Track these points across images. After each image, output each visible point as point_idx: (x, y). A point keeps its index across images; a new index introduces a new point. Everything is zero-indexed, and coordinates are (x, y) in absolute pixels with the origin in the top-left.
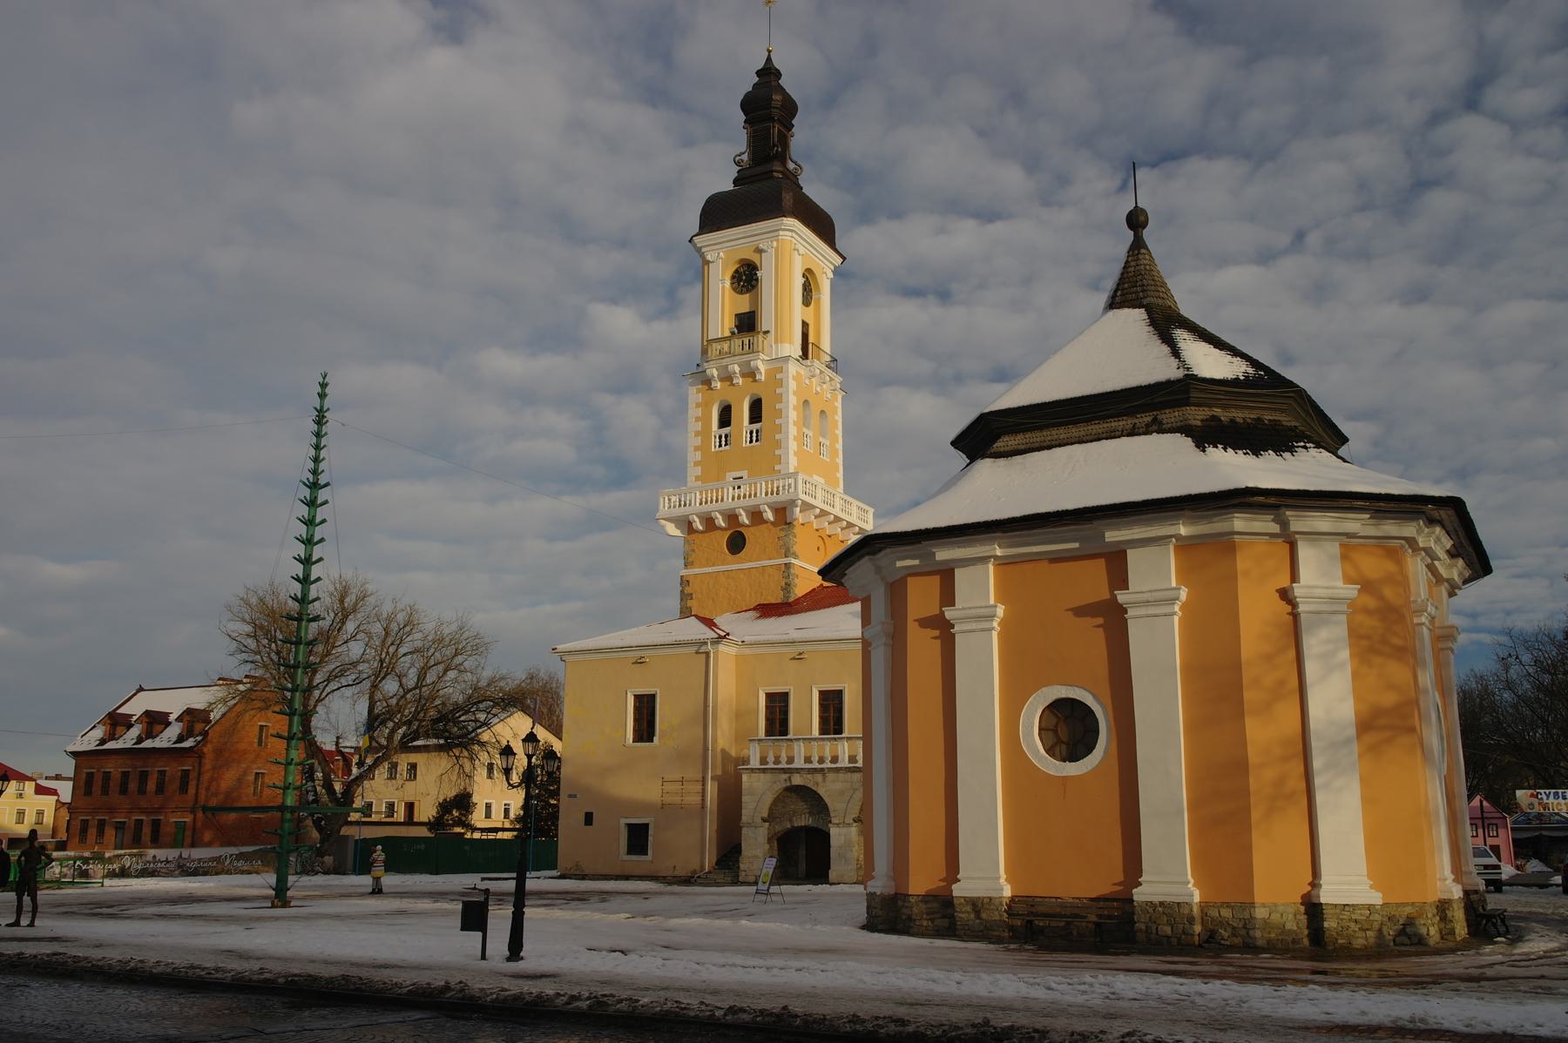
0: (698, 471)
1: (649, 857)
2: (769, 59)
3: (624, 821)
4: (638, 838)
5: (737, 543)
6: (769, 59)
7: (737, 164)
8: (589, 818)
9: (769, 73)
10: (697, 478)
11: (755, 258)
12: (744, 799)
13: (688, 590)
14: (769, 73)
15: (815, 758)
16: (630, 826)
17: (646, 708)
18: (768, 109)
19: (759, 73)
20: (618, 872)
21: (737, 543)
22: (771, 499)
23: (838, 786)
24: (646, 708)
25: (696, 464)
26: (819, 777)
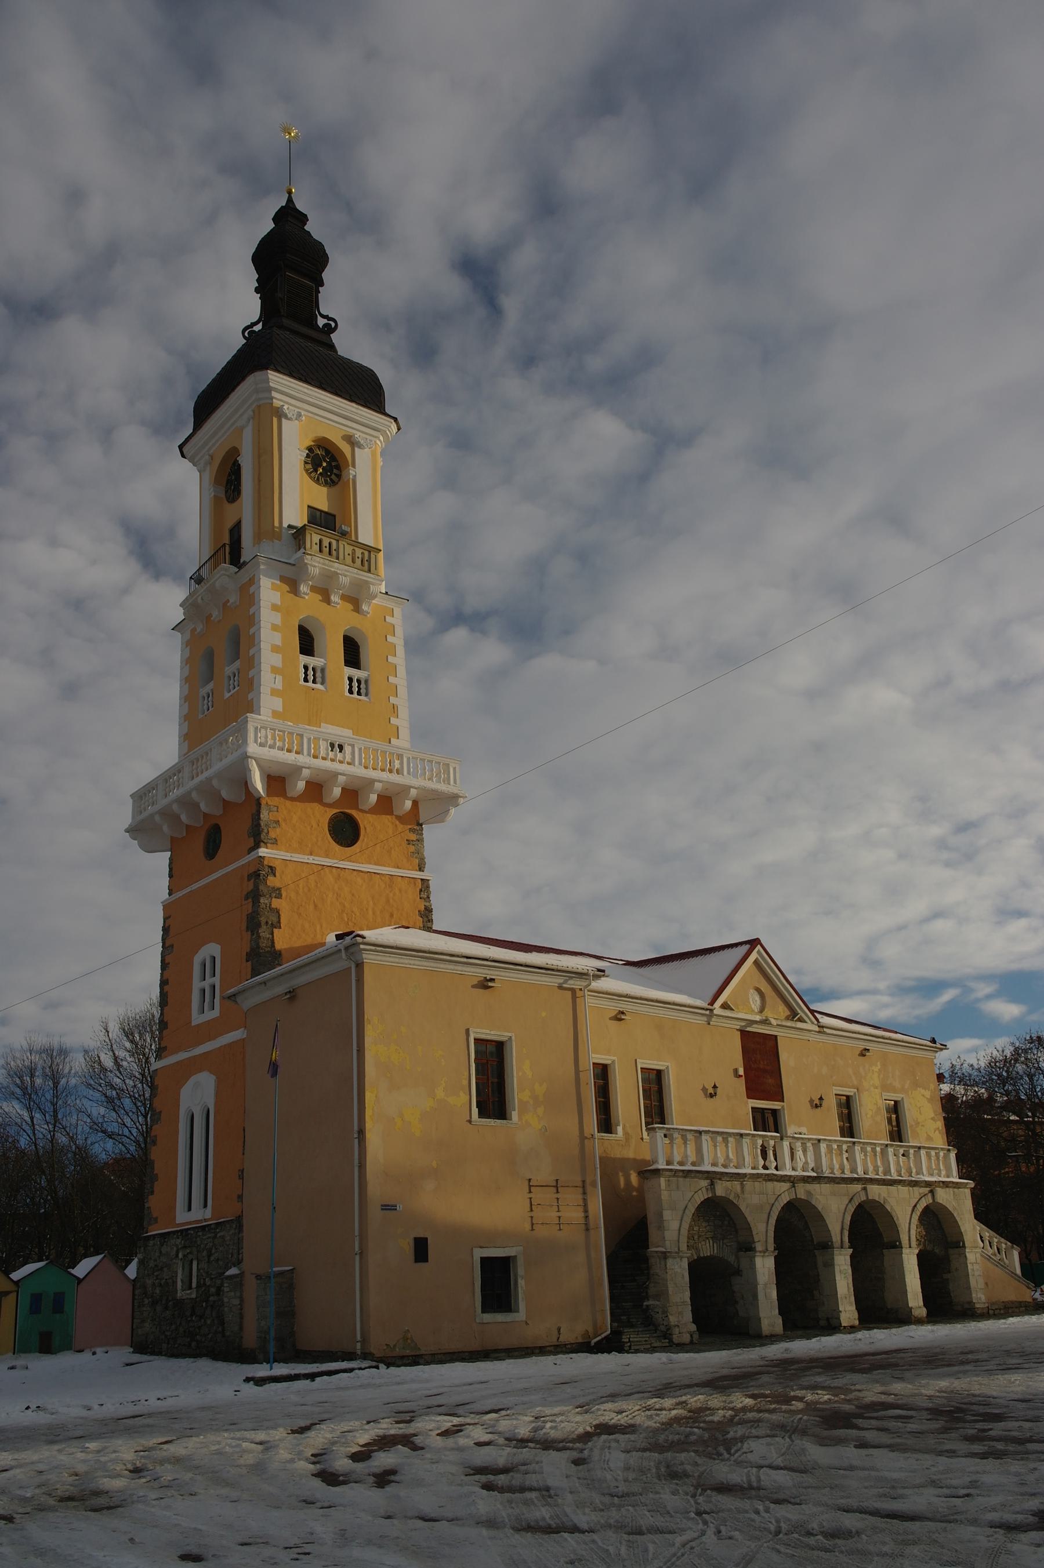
0: (278, 704)
1: (521, 1315)
3: (479, 1253)
4: (497, 1281)
6: (290, 200)
8: (421, 1249)
9: (289, 217)
10: (275, 714)
12: (667, 1215)
13: (272, 881)
14: (289, 217)
15: (721, 1161)
16: (484, 1261)
17: (492, 1063)
20: (475, 1346)
21: (345, 831)
23: (755, 1200)
24: (492, 1063)
25: (274, 692)
26: (737, 1184)
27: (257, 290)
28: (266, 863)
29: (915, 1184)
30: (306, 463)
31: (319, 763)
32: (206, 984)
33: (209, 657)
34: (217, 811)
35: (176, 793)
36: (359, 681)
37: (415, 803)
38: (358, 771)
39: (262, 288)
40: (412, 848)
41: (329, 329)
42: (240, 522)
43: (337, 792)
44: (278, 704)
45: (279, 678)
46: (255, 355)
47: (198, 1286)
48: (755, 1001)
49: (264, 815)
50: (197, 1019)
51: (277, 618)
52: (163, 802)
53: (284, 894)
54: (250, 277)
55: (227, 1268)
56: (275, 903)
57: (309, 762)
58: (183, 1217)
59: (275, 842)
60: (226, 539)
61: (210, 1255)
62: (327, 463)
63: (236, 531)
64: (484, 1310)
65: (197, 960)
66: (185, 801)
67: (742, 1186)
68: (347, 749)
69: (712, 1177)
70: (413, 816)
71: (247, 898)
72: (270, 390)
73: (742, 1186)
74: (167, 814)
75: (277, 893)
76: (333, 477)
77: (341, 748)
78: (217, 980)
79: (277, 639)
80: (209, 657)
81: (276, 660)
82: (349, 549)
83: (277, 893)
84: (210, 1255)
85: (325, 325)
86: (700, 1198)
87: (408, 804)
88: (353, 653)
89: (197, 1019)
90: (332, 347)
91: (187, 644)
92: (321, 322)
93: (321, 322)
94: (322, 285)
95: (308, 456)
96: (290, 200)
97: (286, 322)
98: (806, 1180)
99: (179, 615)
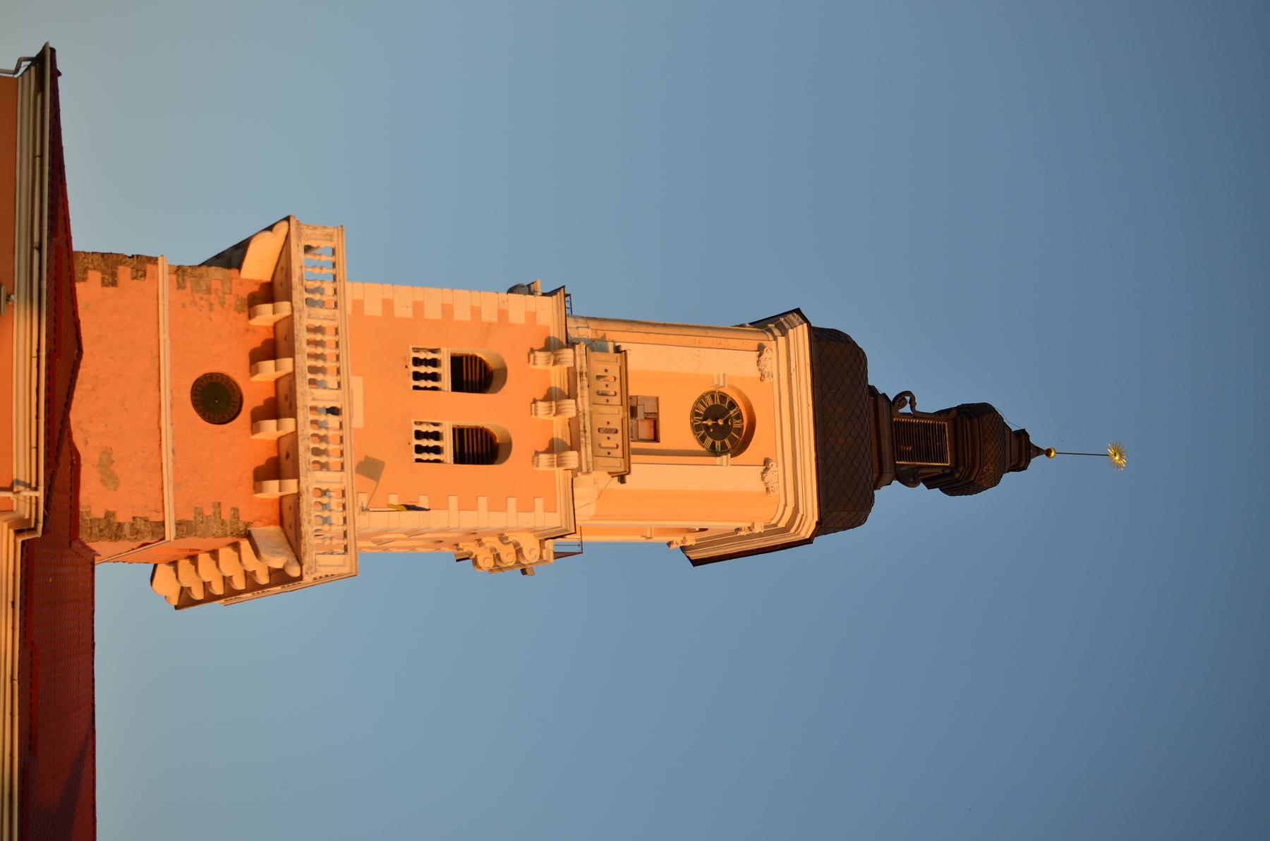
2: (1039, 451)
5: (215, 398)
6: (1039, 451)
7: (901, 398)
9: (1020, 451)
10: (358, 305)
11: (755, 450)
13: (124, 273)
14: (1020, 451)
19: (1022, 434)
21: (215, 398)
22: (308, 501)
28: (149, 267)
31: (302, 336)
38: (307, 397)
44: (373, 309)
45: (409, 313)
51: (489, 315)
53: (111, 290)
59: (180, 286)
72: (784, 333)
76: (709, 440)
79: (462, 314)
81: (433, 312)
82: (616, 424)
88: (479, 448)
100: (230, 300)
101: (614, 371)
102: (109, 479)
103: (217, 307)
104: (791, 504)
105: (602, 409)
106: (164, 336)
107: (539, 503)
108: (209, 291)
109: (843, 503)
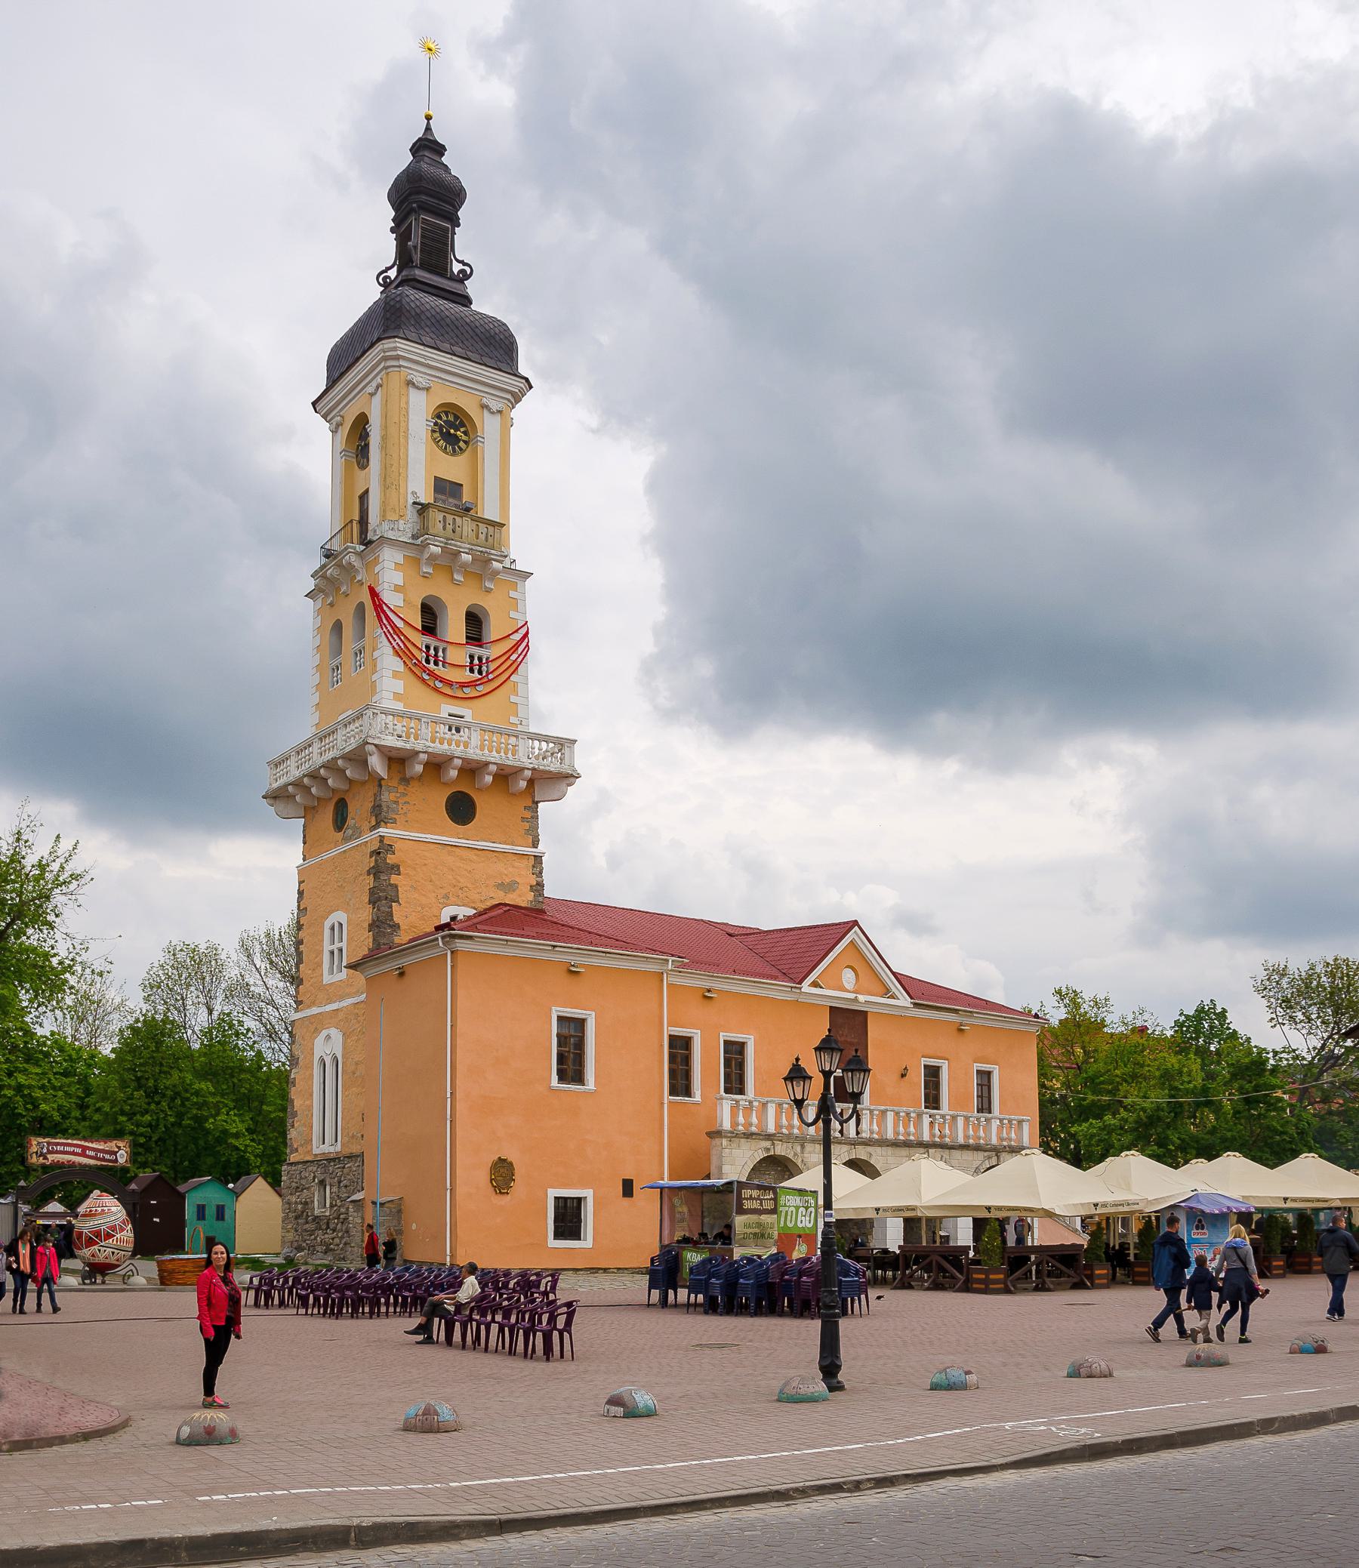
10: (397, 696)
13: (391, 859)
18: (426, 199)
21: (461, 809)
27: (392, 230)
29: (977, 1148)
30: (433, 431)
32: (335, 947)
33: (338, 627)
34: (344, 786)
35: (305, 768)
36: (480, 659)
37: (531, 782)
38: (474, 753)
39: (401, 228)
40: (527, 825)
41: (465, 276)
42: (367, 491)
43: (454, 773)
44: (399, 686)
46: (387, 319)
47: (332, 1206)
48: (848, 977)
49: (387, 797)
50: (327, 979)
52: (295, 773)
54: (387, 213)
55: (353, 1193)
56: (394, 879)
57: (428, 741)
58: (319, 1149)
60: (357, 517)
61: (340, 1182)
62: (453, 429)
63: (364, 497)
64: (558, 1235)
65: (327, 924)
66: (313, 775)
67: (803, 1147)
68: (464, 733)
69: (769, 1137)
70: (533, 785)
71: (369, 873)
73: (803, 1147)
74: (297, 784)
75: (395, 869)
77: (458, 730)
78: (344, 945)
80: (338, 627)
82: (473, 525)
83: (395, 869)
84: (340, 1182)
85: (462, 271)
86: (762, 1155)
87: (523, 784)
89: (327, 979)
90: (466, 301)
91: (319, 612)
92: (456, 268)
93: (456, 268)
94: (459, 225)
95: (436, 424)
96: (428, 129)
97: (420, 274)
98: (868, 1143)
99: (310, 584)
100: (401, 789)
101: (440, 516)
102: (510, 887)
103: (406, 799)
104: (509, 396)
105: (465, 534)
106: (429, 837)
107: (512, 594)
108: (397, 802)
109: (495, 346)
